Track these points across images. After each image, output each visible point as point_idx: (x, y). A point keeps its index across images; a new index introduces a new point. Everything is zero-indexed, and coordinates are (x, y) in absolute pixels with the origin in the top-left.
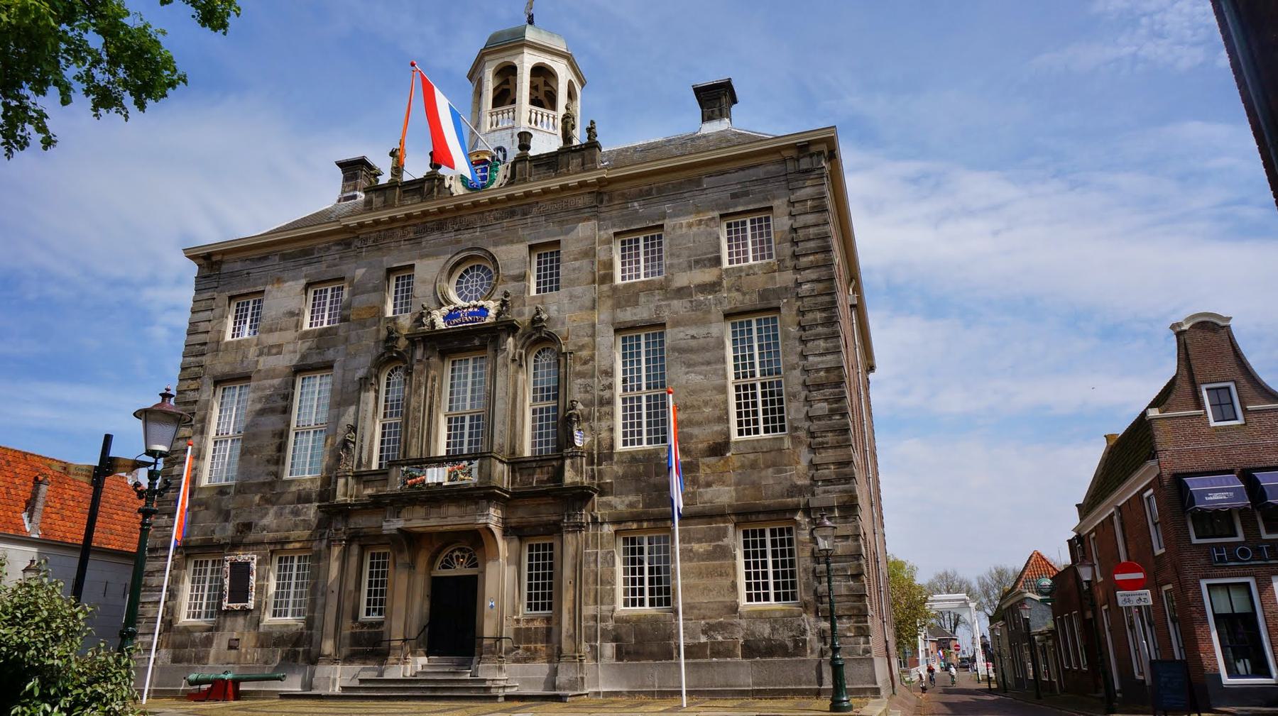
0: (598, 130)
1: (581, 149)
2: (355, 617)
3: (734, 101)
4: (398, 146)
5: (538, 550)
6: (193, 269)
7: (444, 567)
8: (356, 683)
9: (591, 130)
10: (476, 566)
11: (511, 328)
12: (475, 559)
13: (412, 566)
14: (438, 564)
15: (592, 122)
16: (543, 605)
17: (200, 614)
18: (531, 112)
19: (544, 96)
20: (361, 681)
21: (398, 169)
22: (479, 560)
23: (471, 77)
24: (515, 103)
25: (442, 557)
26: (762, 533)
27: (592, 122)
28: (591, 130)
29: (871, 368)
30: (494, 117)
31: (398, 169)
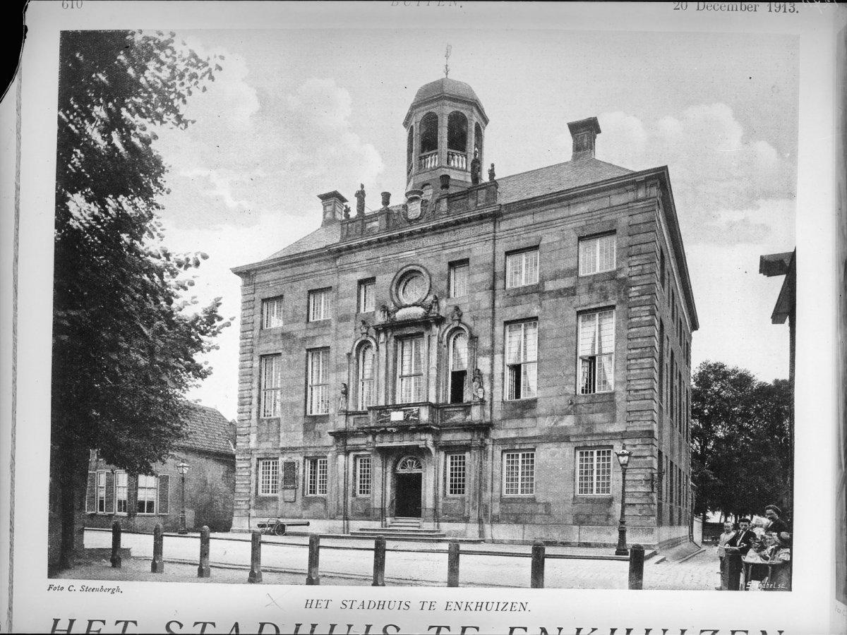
0: (496, 171)
1: (485, 186)
2: (354, 495)
3: (599, 131)
4: (360, 189)
5: (456, 459)
6: (239, 281)
7: (402, 468)
8: (359, 532)
9: (492, 174)
10: (420, 467)
11: (440, 321)
12: (420, 464)
13: (384, 466)
14: (398, 468)
15: (493, 165)
16: (459, 491)
17: (268, 491)
18: (448, 154)
19: (458, 142)
20: (361, 530)
21: (361, 206)
22: (422, 464)
23: (406, 124)
24: (437, 148)
25: (400, 463)
26: (592, 453)
27: (493, 165)
28: (492, 174)
29: (695, 326)
30: (423, 161)
31: (361, 206)
